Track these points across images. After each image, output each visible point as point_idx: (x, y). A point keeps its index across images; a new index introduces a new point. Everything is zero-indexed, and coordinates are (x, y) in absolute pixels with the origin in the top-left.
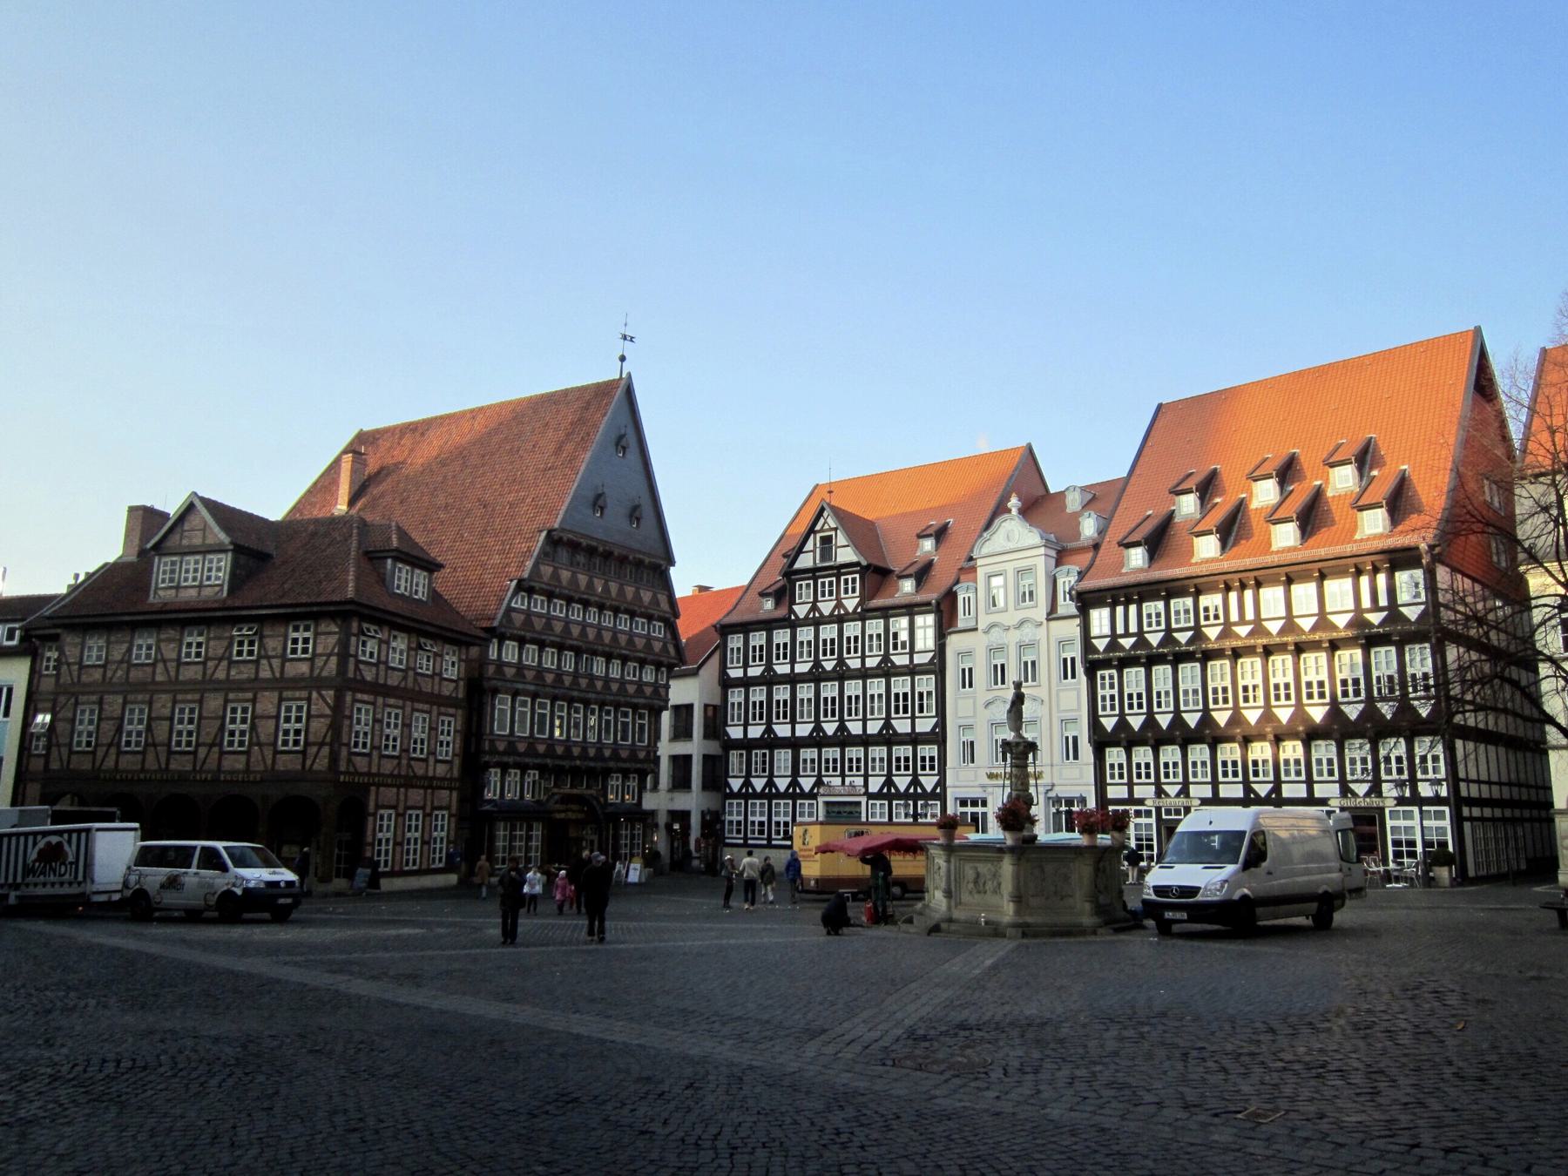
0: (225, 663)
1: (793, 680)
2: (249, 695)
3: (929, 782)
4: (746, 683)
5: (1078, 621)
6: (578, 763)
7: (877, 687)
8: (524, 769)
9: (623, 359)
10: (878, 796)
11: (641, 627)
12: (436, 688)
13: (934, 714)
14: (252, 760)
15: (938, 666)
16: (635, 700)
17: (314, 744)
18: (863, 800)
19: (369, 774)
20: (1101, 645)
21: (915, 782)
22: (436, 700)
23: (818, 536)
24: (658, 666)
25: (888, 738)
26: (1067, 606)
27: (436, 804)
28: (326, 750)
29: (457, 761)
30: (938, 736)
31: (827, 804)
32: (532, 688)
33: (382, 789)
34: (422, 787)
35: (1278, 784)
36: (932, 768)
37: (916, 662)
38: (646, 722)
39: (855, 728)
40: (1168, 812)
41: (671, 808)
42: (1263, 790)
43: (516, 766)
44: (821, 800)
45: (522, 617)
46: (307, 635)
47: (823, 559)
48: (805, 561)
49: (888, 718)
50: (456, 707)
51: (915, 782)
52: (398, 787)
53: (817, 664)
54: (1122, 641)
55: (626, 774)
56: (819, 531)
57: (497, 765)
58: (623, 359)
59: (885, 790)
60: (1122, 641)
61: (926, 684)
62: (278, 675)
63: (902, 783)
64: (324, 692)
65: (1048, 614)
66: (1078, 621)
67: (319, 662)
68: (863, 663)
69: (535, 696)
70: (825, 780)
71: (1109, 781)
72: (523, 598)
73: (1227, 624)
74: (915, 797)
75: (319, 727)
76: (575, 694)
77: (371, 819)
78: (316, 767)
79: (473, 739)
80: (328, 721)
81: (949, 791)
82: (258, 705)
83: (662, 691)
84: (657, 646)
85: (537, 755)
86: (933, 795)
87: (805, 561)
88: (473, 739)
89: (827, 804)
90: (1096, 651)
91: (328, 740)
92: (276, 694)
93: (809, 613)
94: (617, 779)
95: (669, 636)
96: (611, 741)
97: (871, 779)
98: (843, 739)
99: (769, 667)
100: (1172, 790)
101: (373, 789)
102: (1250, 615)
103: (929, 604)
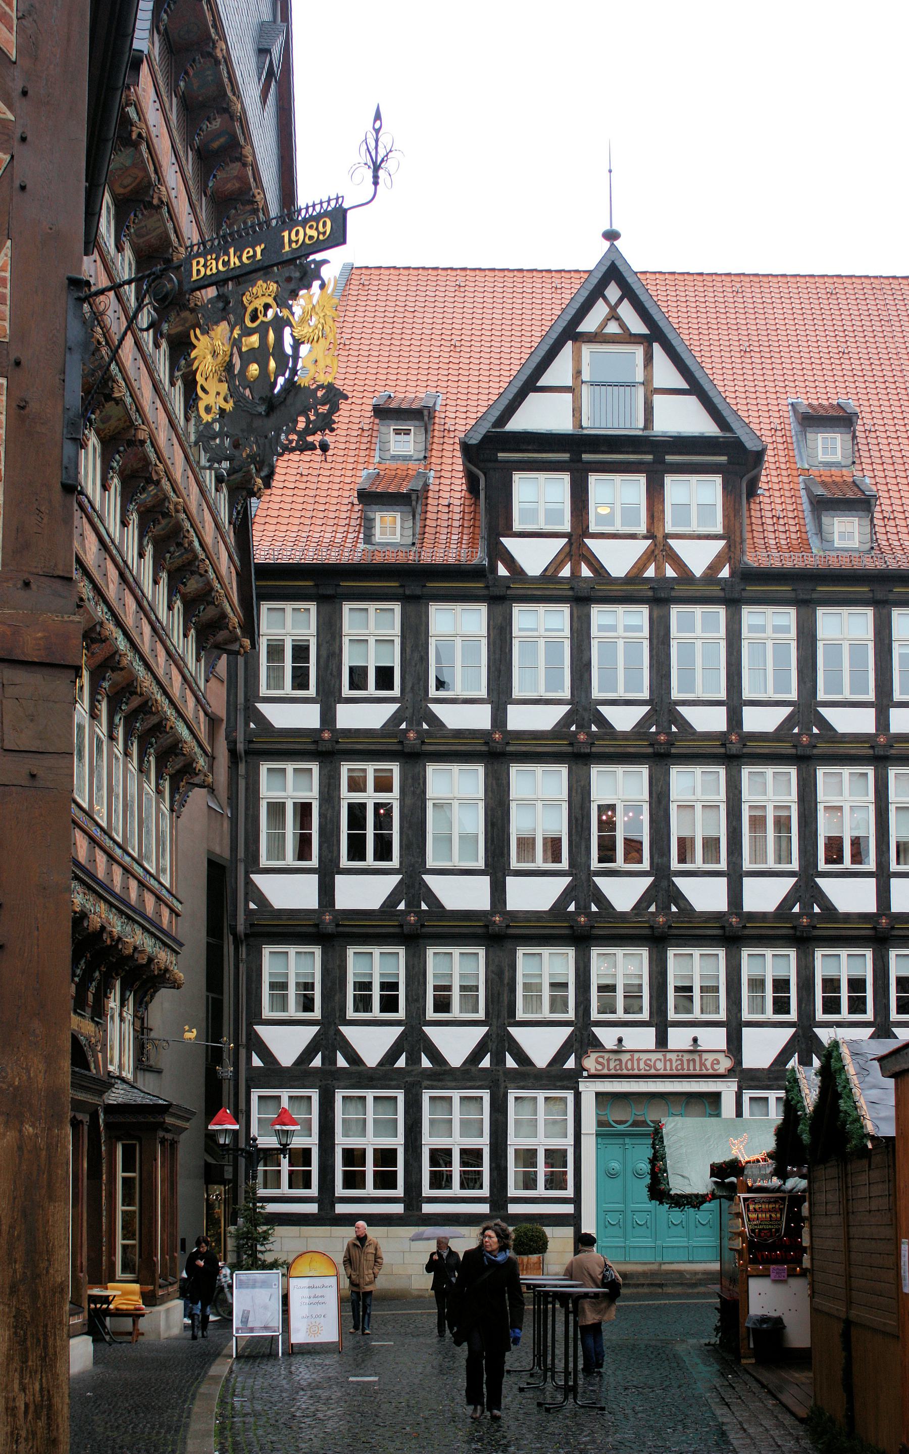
18: (728, 1090)
37: (895, 728)
44: (589, 1089)
70: (607, 1036)
93: (557, 563)
97: (747, 1033)
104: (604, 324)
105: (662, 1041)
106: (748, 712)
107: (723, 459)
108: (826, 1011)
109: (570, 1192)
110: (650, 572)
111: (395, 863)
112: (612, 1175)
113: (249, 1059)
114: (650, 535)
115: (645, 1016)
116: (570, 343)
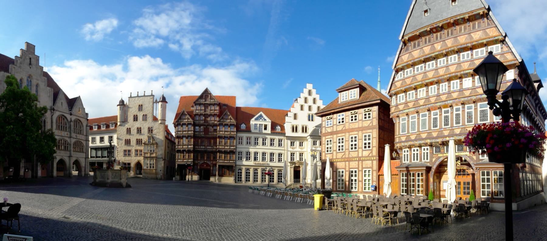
34: (356, 160)
52: (345, 161)
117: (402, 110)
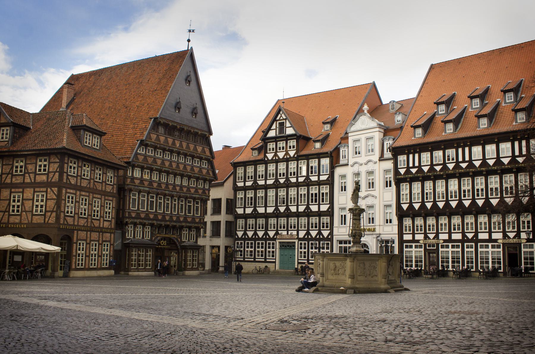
0: (10, 176)
1: (266, 187)
2: (21, 190)
3: (325, 233)
4: (245, 189)
5: (392, 161)
6: (168, 223)
7: (303, 191)
8: (144, 225)
9: (189, 41)
10: (303, 239)
11: (197, 163)
12: (104, 188)
13: (328, 203)
14: (22, 218)
15: (330, 182)
16: (194, 196)
17: (49, 211)
18: (296, 241)
19: (74, 225)
20: (402, 171)
21: (320, 233)
22: (104, 193)
23: (278, 122)
24: (205, 180)
25: (308, 213)
26: (388, 154)
27: (104, 239)
28: (54, 214)
29: (113, 221)
30: (330, 213)
31: (280, 242)
32: (147, 189)
33: (79, 232)
34: (98, 232)
35: (476, 233)
36: (327, 227)
37: (321, 179)
38: (199, 205)
39: (293, 209)
40: (429, 246)
41: (211, 245)
42: (470, 236)
43: (141, 224)
44: (278, 241)
45: (143, 157)
46: (45, 163)
47: (280, 133)
48: (272, 134)
49: (308, 205)
50: (113, 197)
51: (320, 233)
52: (87, 231)
53: (277, 180)
54: (411, 170)
55: (190, 228)
56: (278, 120)
57: (132, 223)
58: (189, 41)
59: (306, 237)
60: (411, 170)
61: (325, 189)
62: (33, 181)
63: (314, 233)
64: (53, 189)
65: (380, 158)
66: (392, 161)
67: (51, 175)
68: (297, 180)
69: (148, 193)
70: (280, 232)
71: (404, 232)
72: (143, 148)
73: (458, 162)
74: (319, 240)
75: (51, 204)
76: (167, 192)
77: (75, 245)
78: (50, 221)
79: (121, 211)
80: (55, 201)
81: (334, 237)
82: (25, 195)
83: (207, 192)
84: (204, 171)
85: (149, 219)
86: (327, 239)
87: (272, 134)
88: (121, 211)
89: (280, 242)
90: (400, 174)
91: (55, 210)
92: (32, 189)
93: (273, 157)
94: (186, 230)
95: (210, 167)
96: (183, 214)
97: (300, 232)
98: (288, 214)
99: (255, 182)
100: (431, 236)
101: (75, 232)
102: (467, 158)
103: (327, 153)
104: (280, 118)
105: (288, 233)
106: (299, 178)
107: (296, 137)
108: (311, 228)
109: (275, 258)
110: (285, 157)
111: (253, 206)
112: (282, 255)
113: (235, 237)
114: (286, 151)
115: (286, 229)
116: (275, 122)
117: (137, 186)
